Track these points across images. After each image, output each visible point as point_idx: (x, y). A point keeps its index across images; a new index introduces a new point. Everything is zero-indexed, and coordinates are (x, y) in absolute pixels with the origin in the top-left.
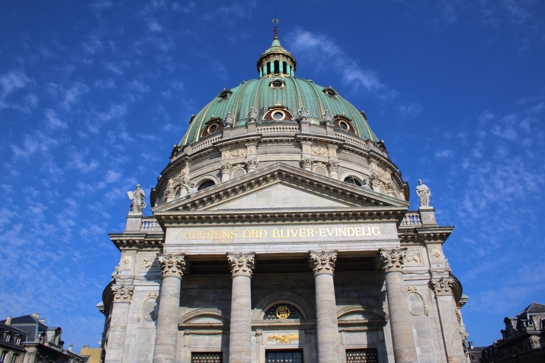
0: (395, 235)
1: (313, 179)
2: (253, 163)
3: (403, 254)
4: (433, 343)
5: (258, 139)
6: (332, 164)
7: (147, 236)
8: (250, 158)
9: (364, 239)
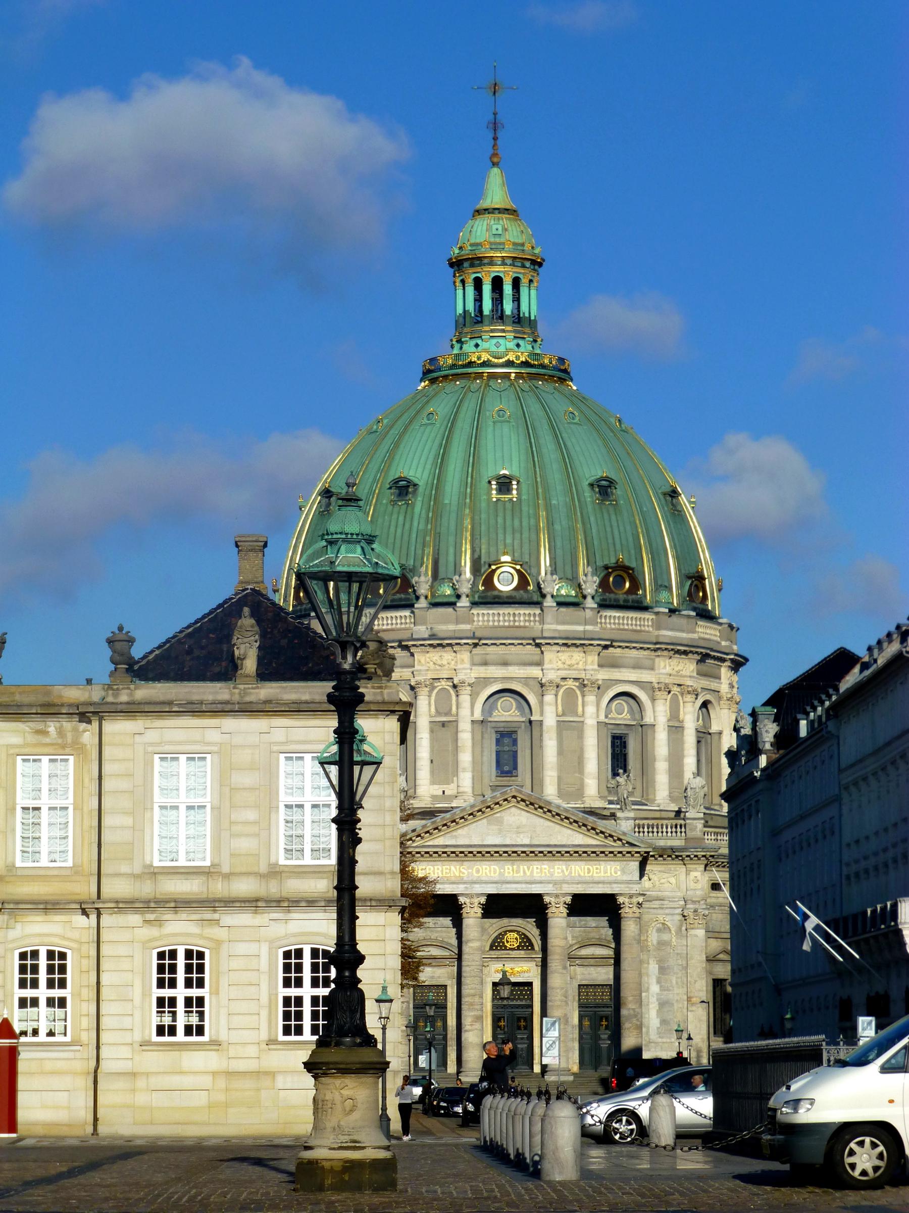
1: (551, 809)
2: (466, 684)
4: (674, 982)
5: (473, 643)
6: (590, 685)
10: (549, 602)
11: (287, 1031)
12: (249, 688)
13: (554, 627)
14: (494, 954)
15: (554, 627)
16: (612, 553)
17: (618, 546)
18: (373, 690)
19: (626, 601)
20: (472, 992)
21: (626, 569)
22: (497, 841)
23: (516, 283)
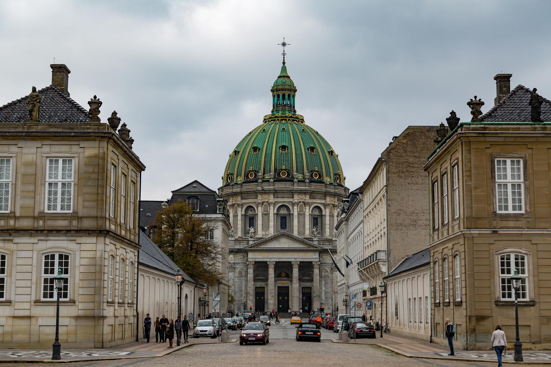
0: (318, 257)
3: (319, 263)
7: (238, 249)
8: (271, 201)
9: (308, 257)
10: (296, 180)
11: (45, 296)
12: (32, 125)
13: (297, 187)
14: (278, 278)
15: (297, 187)
16: (314, 167)
17: (315, 165)
18: (94, 127)
19: (317, 180)
20: (271, 289)
21: (318, 171)
22: (279, 246)
23: (289, 96)
